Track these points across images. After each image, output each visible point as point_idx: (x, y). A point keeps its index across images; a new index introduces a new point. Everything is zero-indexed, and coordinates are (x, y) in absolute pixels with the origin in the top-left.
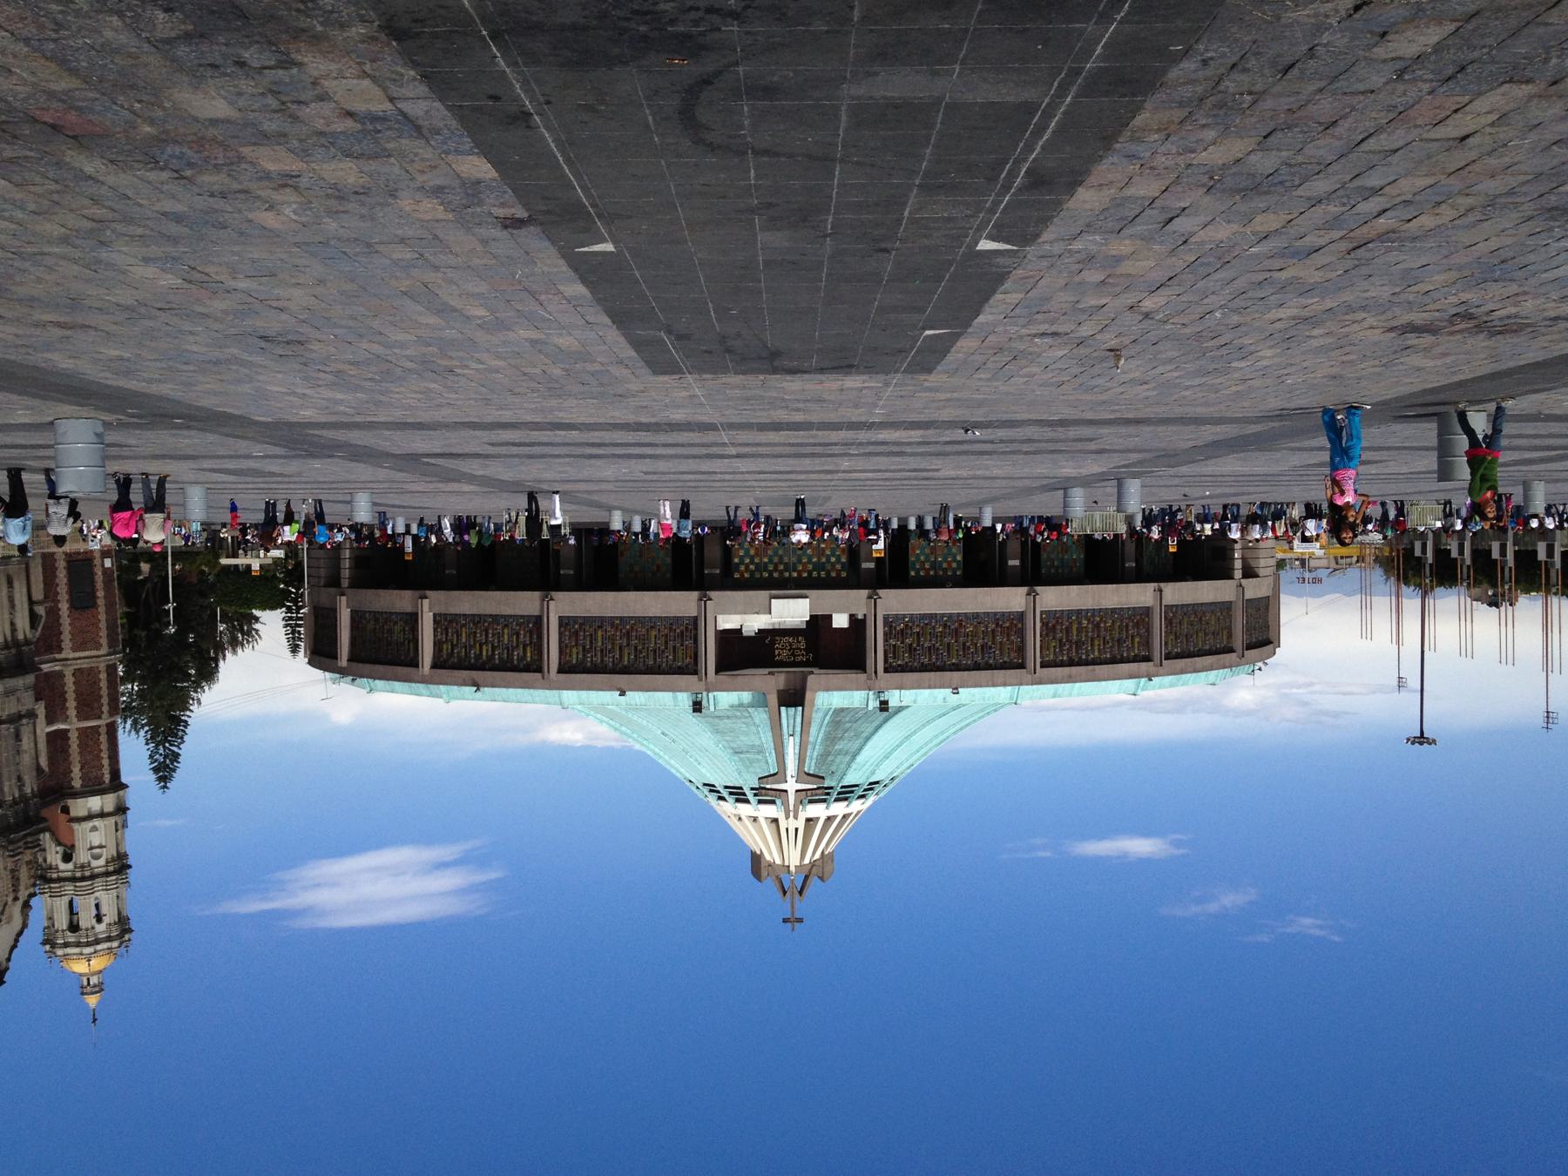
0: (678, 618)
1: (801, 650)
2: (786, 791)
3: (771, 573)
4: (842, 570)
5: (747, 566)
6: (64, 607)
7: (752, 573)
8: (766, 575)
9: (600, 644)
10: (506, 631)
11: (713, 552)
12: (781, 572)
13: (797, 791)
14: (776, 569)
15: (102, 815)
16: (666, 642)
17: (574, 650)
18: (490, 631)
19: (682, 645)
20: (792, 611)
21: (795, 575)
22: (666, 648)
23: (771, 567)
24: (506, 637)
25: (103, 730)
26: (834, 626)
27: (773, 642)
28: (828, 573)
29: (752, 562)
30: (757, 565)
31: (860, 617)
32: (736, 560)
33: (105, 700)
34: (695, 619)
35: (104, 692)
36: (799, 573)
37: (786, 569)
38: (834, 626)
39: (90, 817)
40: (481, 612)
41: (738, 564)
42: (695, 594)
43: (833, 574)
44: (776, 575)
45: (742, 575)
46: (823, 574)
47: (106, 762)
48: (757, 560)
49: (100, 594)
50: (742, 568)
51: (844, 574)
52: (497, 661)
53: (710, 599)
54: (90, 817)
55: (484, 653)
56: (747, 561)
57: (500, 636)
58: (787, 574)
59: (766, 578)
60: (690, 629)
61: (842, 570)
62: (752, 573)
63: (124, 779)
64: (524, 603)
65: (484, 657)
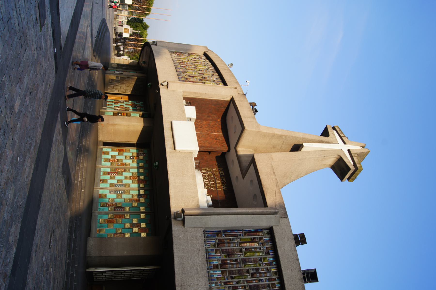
0: (209, 257)
2: (349, 151)
5: (133, 225)
8: (142, 209)
13: (345, 143)
16: (240, 272)
22: (248, 272)
31: (184, 102)
32: (128, 235)
34: (206, 232)
44: (142, 200)
45: (143, 230)
50: (135, 230)
53: (183, 211)
56: (128, 225)
59: (145, 209)
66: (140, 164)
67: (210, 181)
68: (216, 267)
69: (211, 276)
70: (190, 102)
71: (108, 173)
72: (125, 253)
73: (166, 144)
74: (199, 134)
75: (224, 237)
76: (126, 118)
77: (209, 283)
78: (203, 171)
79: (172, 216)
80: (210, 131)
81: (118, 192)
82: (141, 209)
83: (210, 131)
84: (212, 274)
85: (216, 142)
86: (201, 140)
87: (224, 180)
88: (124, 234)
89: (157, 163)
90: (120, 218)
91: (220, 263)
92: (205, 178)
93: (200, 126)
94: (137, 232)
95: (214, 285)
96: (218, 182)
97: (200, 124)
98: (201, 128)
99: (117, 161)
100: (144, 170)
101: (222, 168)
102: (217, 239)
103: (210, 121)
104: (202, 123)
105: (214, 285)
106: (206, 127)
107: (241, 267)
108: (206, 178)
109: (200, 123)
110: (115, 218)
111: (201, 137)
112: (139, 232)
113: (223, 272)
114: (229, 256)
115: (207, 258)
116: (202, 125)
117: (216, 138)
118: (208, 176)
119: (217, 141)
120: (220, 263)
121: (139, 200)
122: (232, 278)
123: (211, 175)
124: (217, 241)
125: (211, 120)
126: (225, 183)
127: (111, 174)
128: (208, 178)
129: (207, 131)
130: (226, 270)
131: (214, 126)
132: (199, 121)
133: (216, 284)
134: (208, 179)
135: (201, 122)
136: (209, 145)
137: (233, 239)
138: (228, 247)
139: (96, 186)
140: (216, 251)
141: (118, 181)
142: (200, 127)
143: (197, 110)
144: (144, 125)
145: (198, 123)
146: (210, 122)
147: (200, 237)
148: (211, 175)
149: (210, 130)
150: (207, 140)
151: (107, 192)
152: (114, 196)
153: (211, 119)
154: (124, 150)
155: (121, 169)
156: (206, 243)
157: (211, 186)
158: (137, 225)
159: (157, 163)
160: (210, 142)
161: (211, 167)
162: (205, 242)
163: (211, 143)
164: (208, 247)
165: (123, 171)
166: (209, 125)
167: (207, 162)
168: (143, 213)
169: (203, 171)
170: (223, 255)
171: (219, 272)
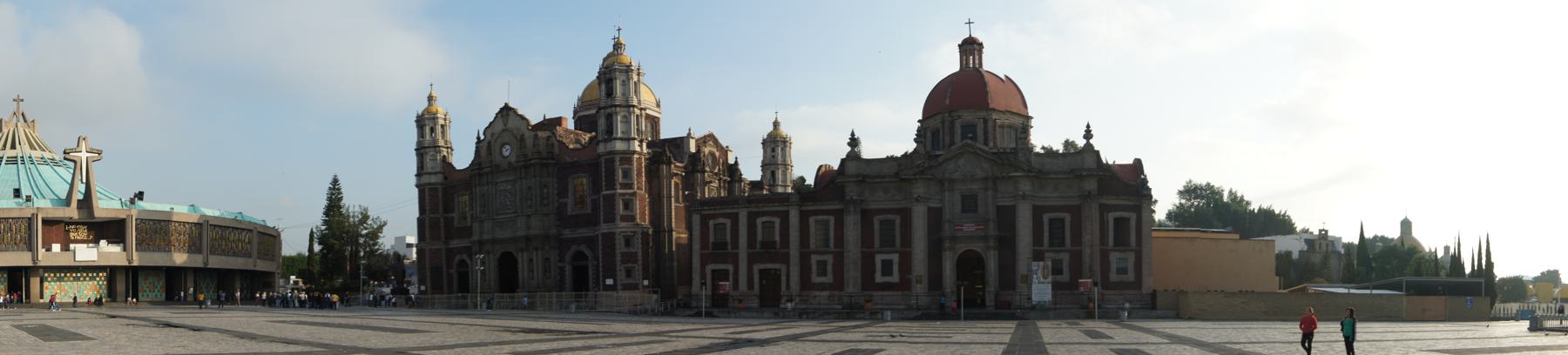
0: (145, 250)
3: (87, 276)
4: (47, 278)
5: (101, 280)
6: (445, 269)
7: (98, 276)
8: (90, 275)
11: (121, 287)
12: (82, 276)
14: (85, 278)
15: (430, 174)
20: (85, 253)
21: (74, 275)
23: (87, 279)
25: (427, 212)
26: (59, 245)
27: (88, 236)
28: (55, 275)
33: (427, 225)
35: (427, 229)
36: (71, 276)
37: (79, 277)
38: (59, 245)
39: (435, 173)
40: (234, 258)
43: (52, 275)
44: (85, 275)
46: (58, 275)
47: (427, 198)
49: (428, 274)
51: (46, 275)
54: (435, 173)
56: (101, 283)
57: (226, 245)
58: (79, 275)
60: (142, 245)
61: (47, 278)
62: (98, 276)
63: (416, 190)
64: (216, 262)
158: (101, 277)
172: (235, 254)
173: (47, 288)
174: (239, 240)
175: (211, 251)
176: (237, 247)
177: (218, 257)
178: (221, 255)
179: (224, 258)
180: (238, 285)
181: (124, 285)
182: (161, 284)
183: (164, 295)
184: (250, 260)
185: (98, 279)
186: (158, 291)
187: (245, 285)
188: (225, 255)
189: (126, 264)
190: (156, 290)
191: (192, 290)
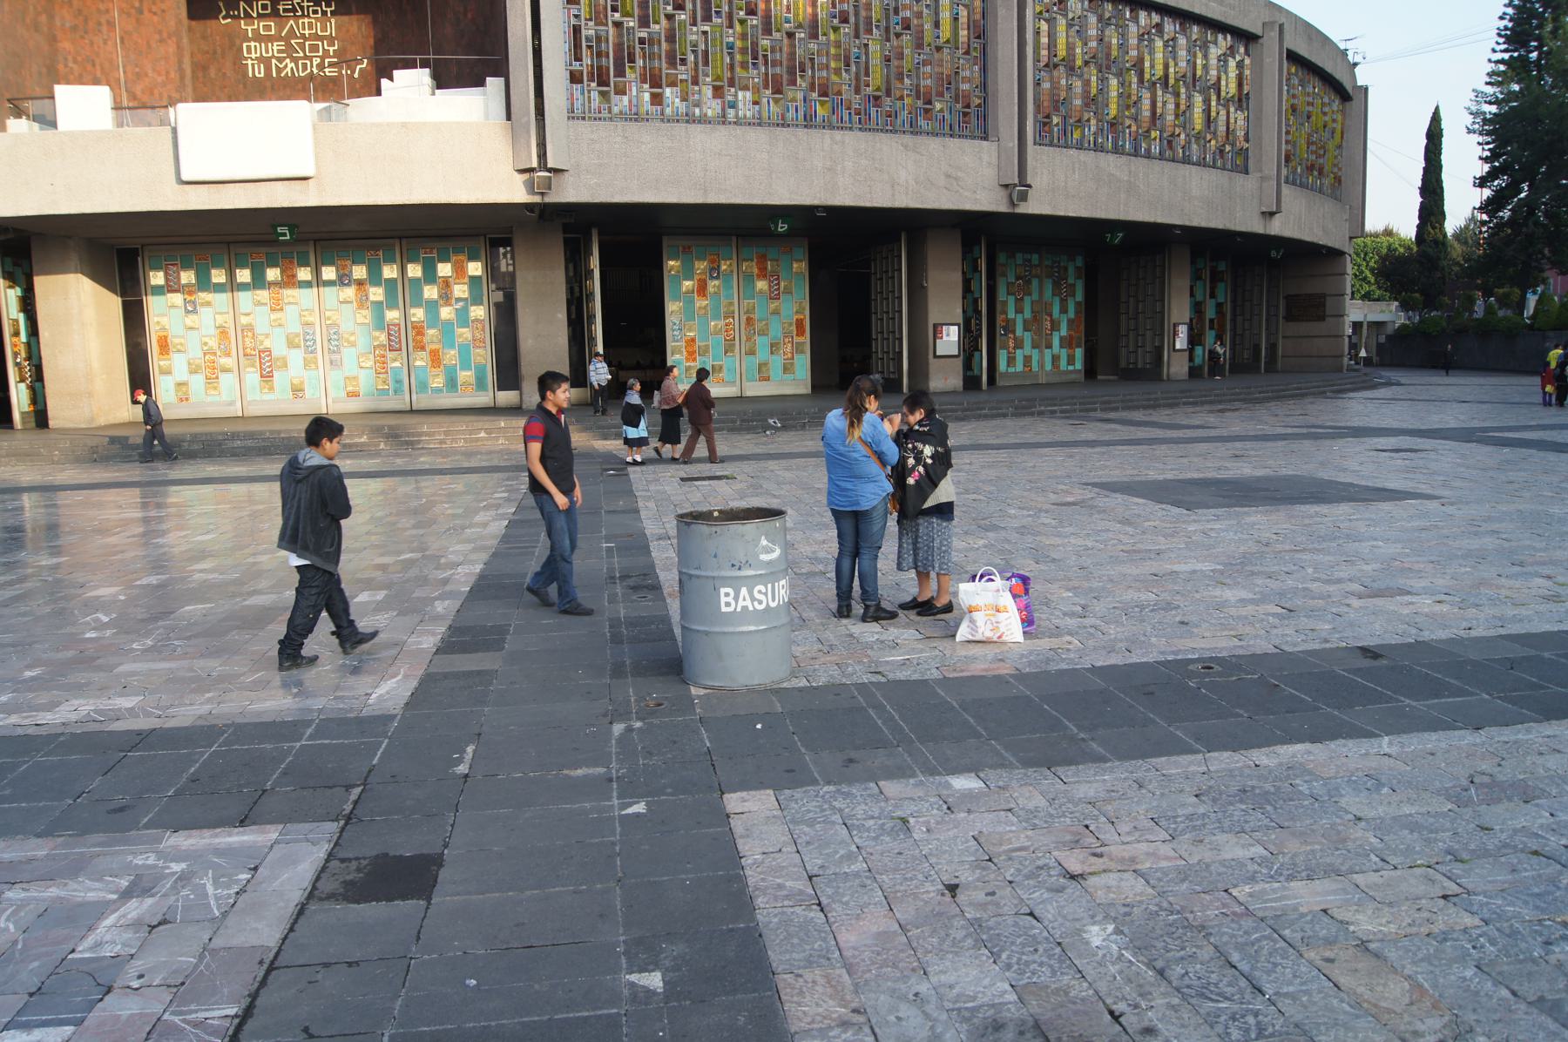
0: (636, 117)
1: (258, 38)
5: (446, 297)
7: (430, 275)
8: (390, 272)
9: (874, 48)
10: (1113, 110)
16: (671, 38)
17: (946, 31)
18: (1147, 114)
19: (618, 25)
24: (1114, 94)
26: (101, 96)
27: (344, 59)
29: (432, 307)
30: (418, 300)
32: (479, 312)
41: (476, 300)
42: (571, 192)
45: (460, 270)
48: (418, 314)
50: (460, 290)
52: (1133, 28)
55: (1159, 56)
56: (446, 313)
59: (390, 260)
62: (430, 275)
65: (1159, 44)
66: (215, 280)
67: (301, 54)
68: (657, 99)
69: (678, 115)
70: (8, 100)
71: (267, 377)
72: (560, 316)
73: (285, 205)
74: (125, 72)
75: (581, 65)
76: (46, 334)
77: (694, 121)
78: (260, 73)
79: (537, 199)
80: (105, 29)
81: (336, 343)
82: (390, 276)
83: (105, 29)
84: (673, 112)
85: (155, 14)
86: (154, 70)
87: (293, 5)
88: (473, 321)
89: (279, 230)
90: (423, 334)
91: (646, 86)
92: (289, 69)
93: (89, 67)
94: (465, 287)
95: (697, 111)
96: (304, 29)
97: (75, 67)
98: (97, 61)
99: (215, 354)
100: (243, 267)
101: (242, 3)
102: (588, 85)
103: (58, 23)
104: (70, 58)
105: (697, 111)
106: (87, 41)
107: (660, 33)
108: (290, 66)
109: (71, 65)
110: (423, 348)
111: (137, 70)
112: (466, 280)
113: (673, 84)
114: (632, 60)
115: (636, 120)
116: (79, 59)
117: (133, 11)
118: (280, 60)
119: (150, 11)
120: (646, 86)
121: (360, 283)
122: (683, 62)
123: (275, 48)
124: (594, 85)
125: (51, 17)
126: (305, 4)
127: (268, 370)
128: (288, 60)
129: (105, 42)
130: (667, 74)
131: (80, 11)
132: (61, 67)
133: (697, 105)
134: (295, 60)
135: (66, 59)
136: (170, 42)
137: (588, 39)
138: (608, 57)
139: (320, 408)
140: (621, 91)
141: (291, 344)
142: (94, 65)
143: (214, 98)
144: (76, 272)
145: (72, 73)
146: (63, 25)
147: (592, 132)
148: (275, 48)
149: (99, 31)
150: (149, 46)
151: (336, 377)
152: (349, 355)
153: (43, 18)
154: (162, 334)
155: (244, 342)
156: (598, 115)
157: (321, 54)
158: (446, 283)
159: (279, 230)
160: (157, 37)
161: (238, 42)
162: (595, 119)
163: (160, 32)
164: (610, 112)
165: (250, 334)
166: (74, 28)
167: (215, 52)
168: (403, 271)
169: (260, 73)
170: (630, 76)
171: (668, 91)
172: (1170, 152)
173: (164, 346)
174: (1192, 80)
175: (1044, 124)
176: (1182, 114)
177: (1088, 157)
178: (1098, 148)
179: (1112, 164)
180: (1179, 311)
181: (562, 316)
182: (795, 305)
183: (803, 364)
184: (1246, 185)
185: (431, 292)
186: (774, 348)
187: (1210, 313)
188: (1117, 150)
189: (514, 191)
190: (762, 342)
191: (950, 339)
